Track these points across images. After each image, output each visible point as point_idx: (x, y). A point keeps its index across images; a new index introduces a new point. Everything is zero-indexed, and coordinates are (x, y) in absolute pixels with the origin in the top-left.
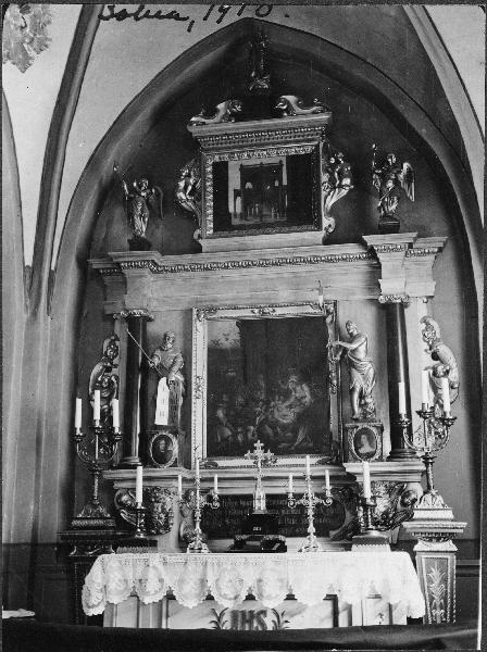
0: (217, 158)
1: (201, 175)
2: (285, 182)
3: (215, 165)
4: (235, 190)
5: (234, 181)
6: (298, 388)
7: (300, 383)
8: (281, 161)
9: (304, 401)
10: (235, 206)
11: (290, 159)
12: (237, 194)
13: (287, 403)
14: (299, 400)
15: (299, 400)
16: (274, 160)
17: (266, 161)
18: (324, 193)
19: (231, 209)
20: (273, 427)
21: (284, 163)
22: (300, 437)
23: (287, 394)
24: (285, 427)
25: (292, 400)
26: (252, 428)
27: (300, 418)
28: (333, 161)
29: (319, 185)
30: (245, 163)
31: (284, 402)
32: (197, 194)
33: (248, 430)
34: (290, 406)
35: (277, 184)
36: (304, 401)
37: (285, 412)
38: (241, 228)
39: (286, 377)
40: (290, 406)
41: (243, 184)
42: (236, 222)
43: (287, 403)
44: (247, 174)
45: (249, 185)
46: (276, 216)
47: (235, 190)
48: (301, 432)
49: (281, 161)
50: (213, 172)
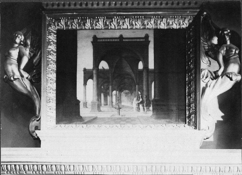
0: (62, 24)
1: (38, 46)
2: (151, 66)
3: (60, 33)
4: (85, 70)
5: (85, 58)
8: (147, 36)
10: (86, 92)
11: (157, 32)
12: (88, 75)
16: (141, 34)
17: (127, 34)
18: (203, 85)
19: (80, 96)
21: (151, 39)
28: (215, 41)
29: (197, 70)
30: (100, 35)
32: (34, 70)
35: (141, 66)
38: (93, 120)
41: (96, 63)
42: (84, 112)
44: (102, 49)
45: (104, 65)
46: (139, 109)
47: (85, 70)
49: (147, 36)
50: (59, 45)
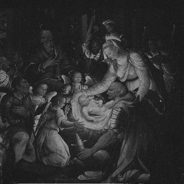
6: (122, 61)
7: (125, 48)
9: (132, 87)
13: (101, 89)
14: (124, 84)
15: (124, 84)
20: (68, 136)
22: (123, 159)
23: (99, 70)
24: (91, 138)
25: (109, 82)
26: (25, 136)
27: (123, 119)
31: (90, 86)
33: (18, 141)
34: (105, 97)
36: (132, 87)
37: (94, 106)
39: (97, 44)
40: (105, 97)
43: (101, 89)
48: (125, 147)
